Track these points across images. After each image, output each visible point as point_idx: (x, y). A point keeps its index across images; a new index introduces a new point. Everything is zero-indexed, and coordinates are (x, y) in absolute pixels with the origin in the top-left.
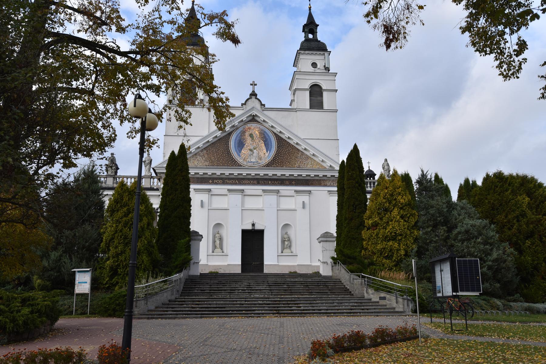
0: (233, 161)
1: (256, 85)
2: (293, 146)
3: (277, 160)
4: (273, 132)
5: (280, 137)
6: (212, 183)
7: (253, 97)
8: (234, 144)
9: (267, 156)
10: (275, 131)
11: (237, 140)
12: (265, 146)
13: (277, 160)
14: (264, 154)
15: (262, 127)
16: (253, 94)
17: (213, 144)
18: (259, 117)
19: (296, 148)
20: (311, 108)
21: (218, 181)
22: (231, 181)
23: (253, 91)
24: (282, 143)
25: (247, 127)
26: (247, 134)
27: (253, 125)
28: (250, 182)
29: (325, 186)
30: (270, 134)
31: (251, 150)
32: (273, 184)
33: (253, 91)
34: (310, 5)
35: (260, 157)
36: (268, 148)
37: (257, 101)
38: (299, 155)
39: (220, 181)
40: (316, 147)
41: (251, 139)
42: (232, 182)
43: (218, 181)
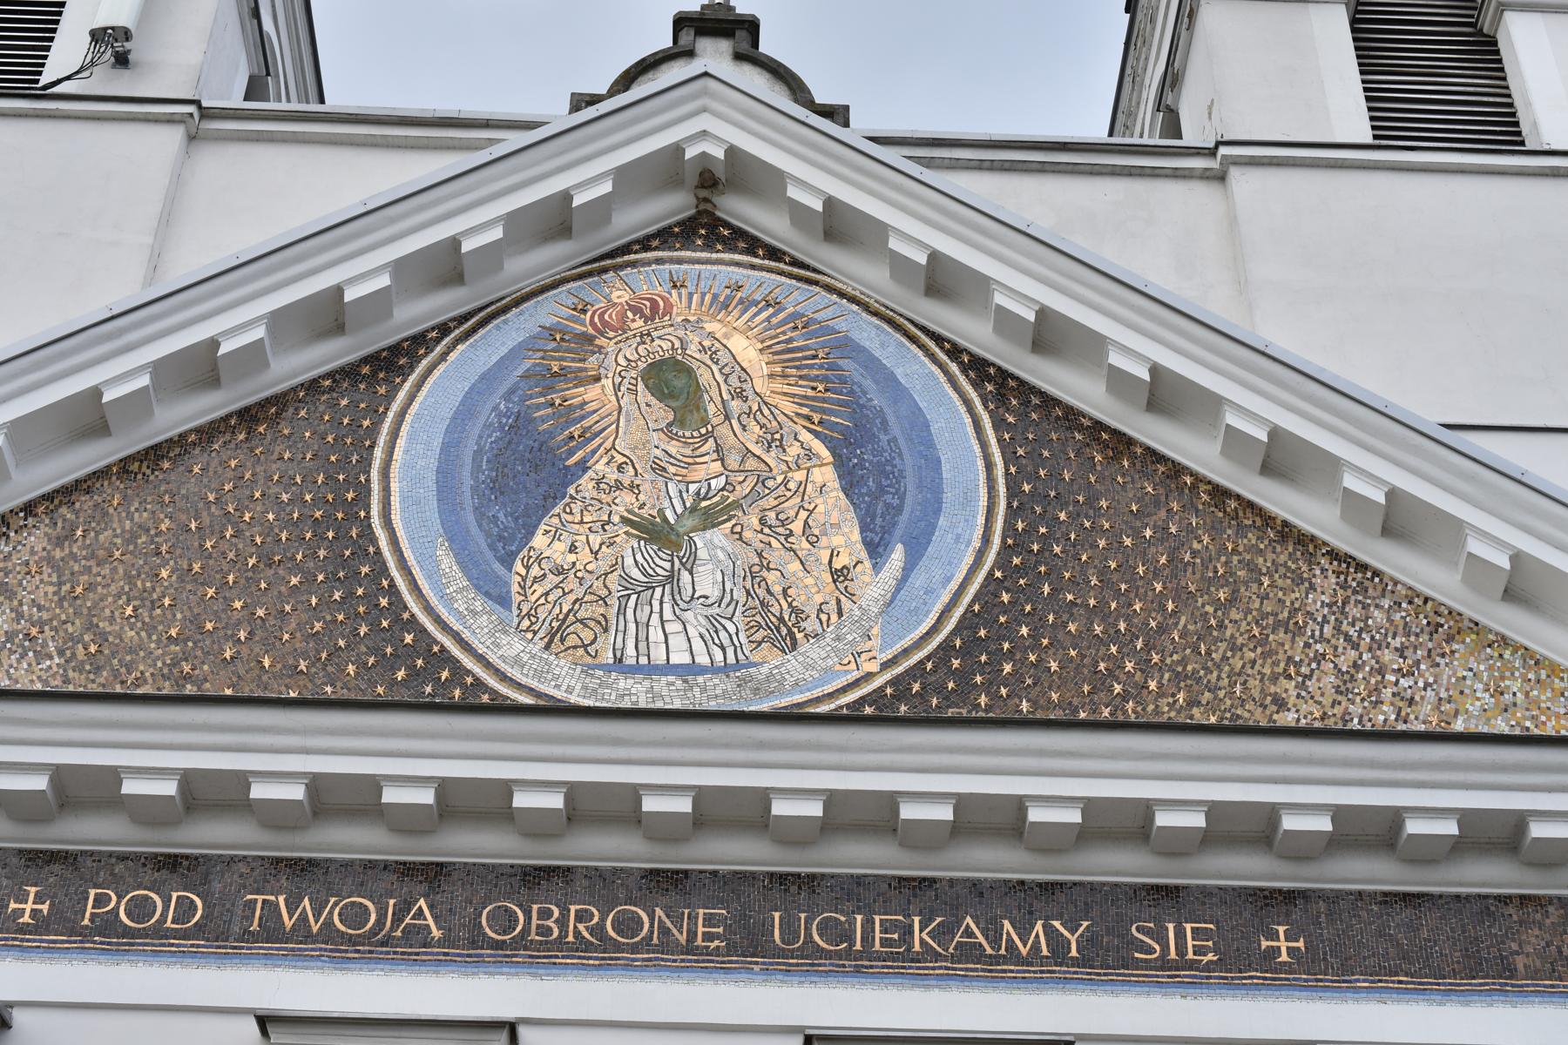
0: (404, 655)
2: (1220, 494)
3: (1019, 646)
4: (955, 352)
5: (1049, 401)
6: (41, 925)
7: (714, 56)
8: (429, 464)
10: (975, 333)
11: (485, 415)
12: (850, 483)
13: (1019, 646)
14: (840, 575)
15: (798, 298)
17: (154, 454)
19: (1267, 519)
21: (140, 909)
22: (334, 912)
25: (621, 296)
28: (628, 925)
31: (655, 532)
32: (969, 953)
35: (779, 607)
38: (1315, 602)
39: (163, 907)
41: (662, 414)
42: (355, 916)
43: (140, 909)
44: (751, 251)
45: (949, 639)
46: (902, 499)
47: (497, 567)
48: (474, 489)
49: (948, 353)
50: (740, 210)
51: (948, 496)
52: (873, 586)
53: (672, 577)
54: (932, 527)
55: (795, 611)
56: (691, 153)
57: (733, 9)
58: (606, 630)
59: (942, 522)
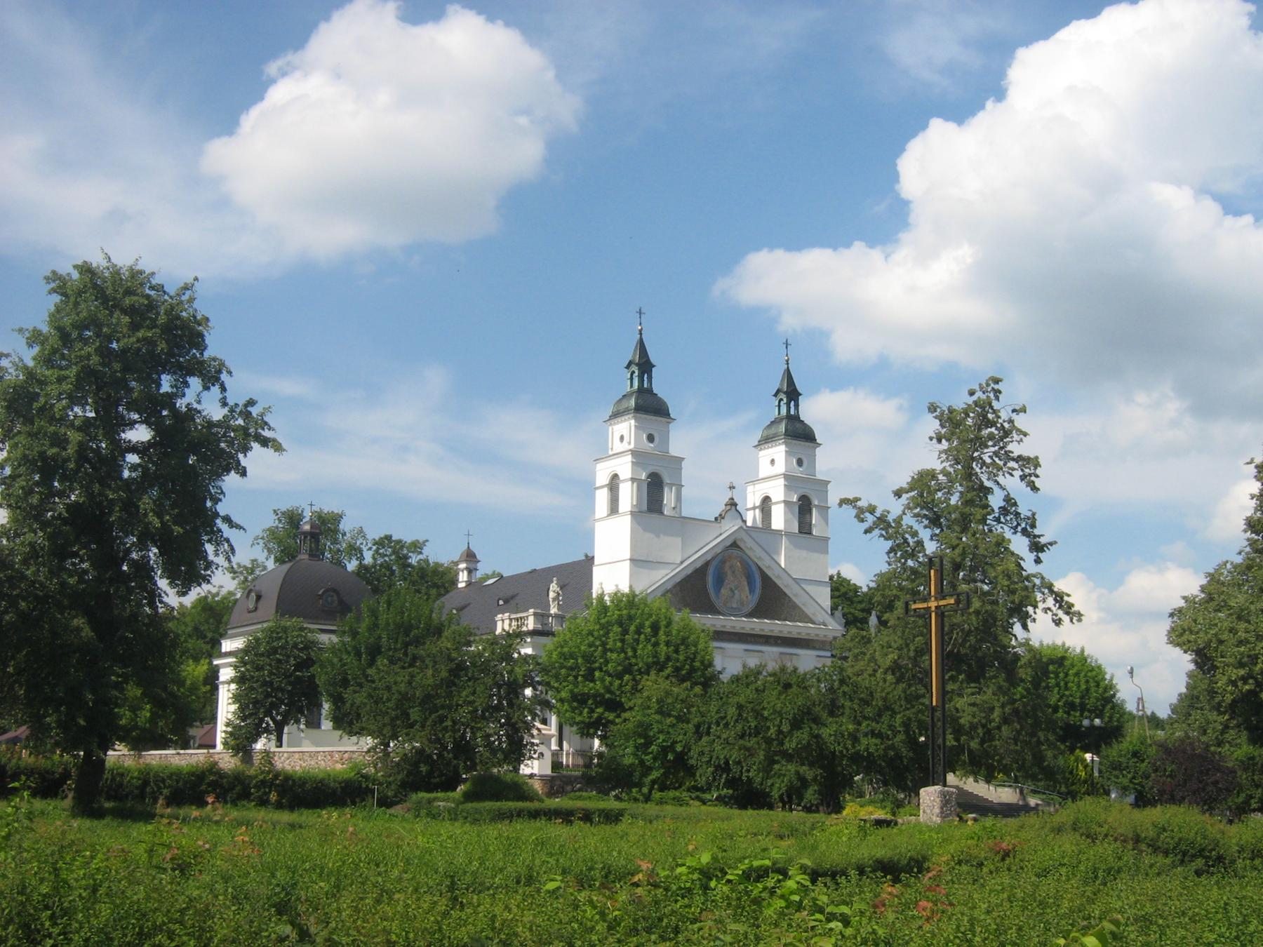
1: (734, 488)
9: (752, 600)
10: (760, 564)
12: (748, 583)
16: (732, 504)
18: (745, 542)
20: (800, 532)
24: (768, 583)
26: (728, 564)
27: (735, 552)
29: (814, 648)
30: (754, 568)
33: (732, 499)
34: (787, 355)
36: (752, 590)
37: (736, 512)
40: (810, 593)
50: (739, 543)
52: (749, 597)
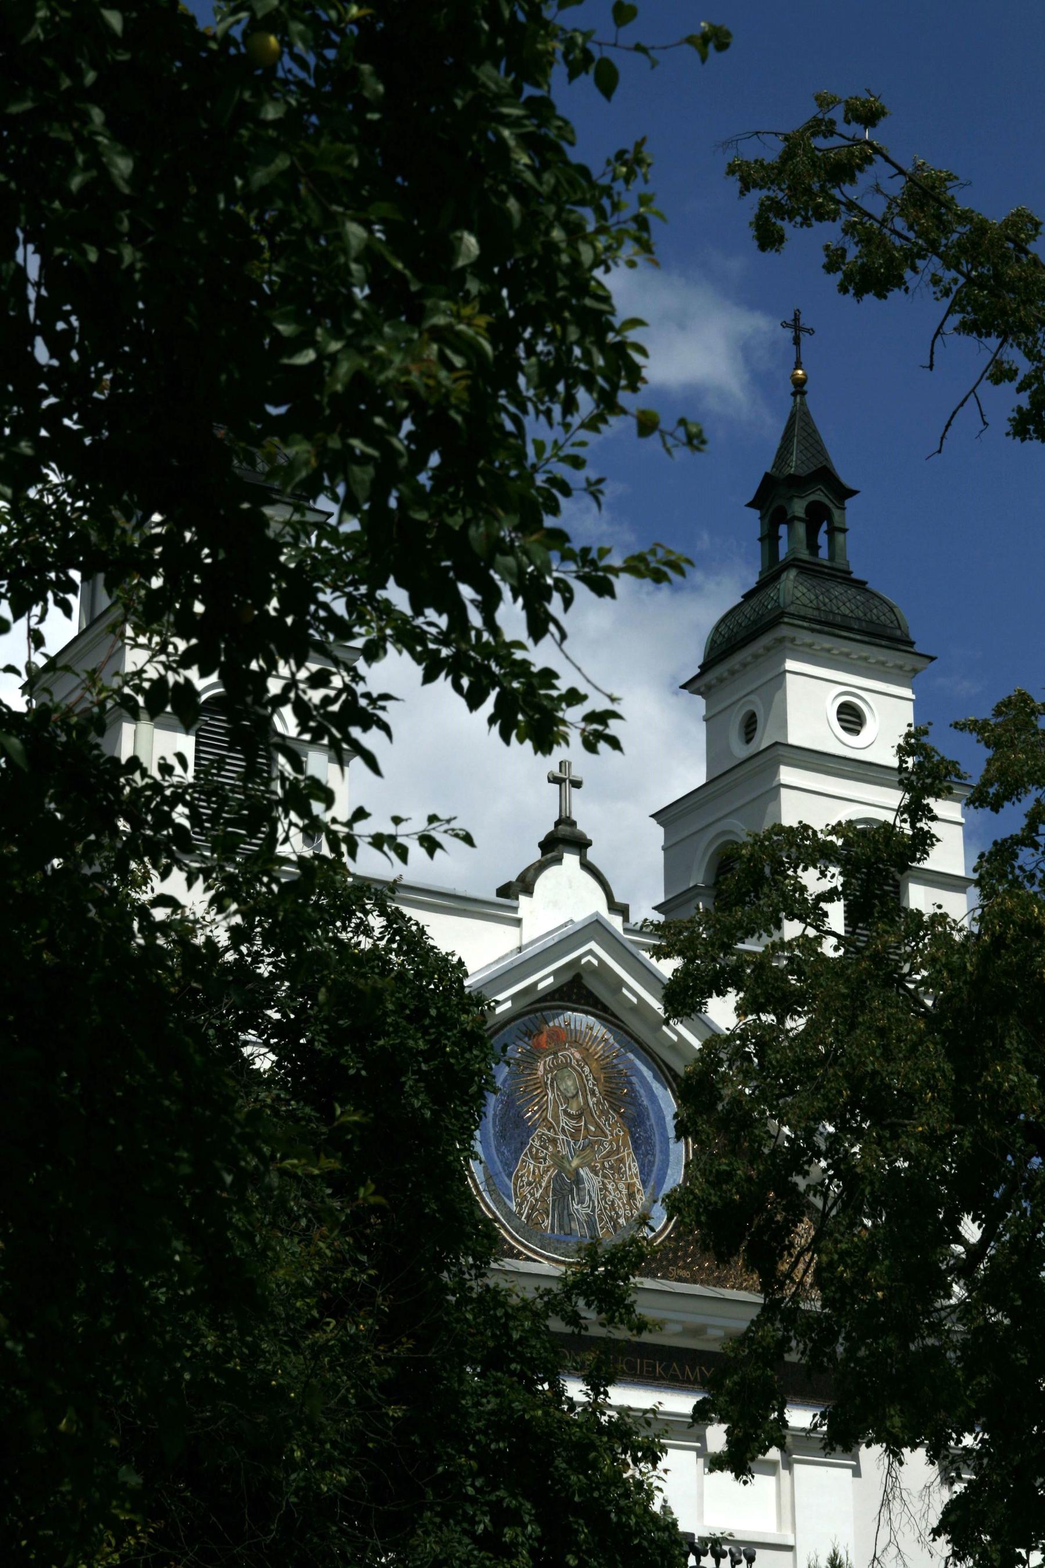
1: (577, 784)
12: (636, 1149)
14: (631, 1196)
23: (565, 821)
33: (565, 821)
44: (595, 1006)
45: (670, 1233)
46: (654, 1155)
47: (506, 1179)
48: (495, 1135)
49: (673, 1077)
51: (671, 1158)
53: (571, 1191)
54: (665, 1173)
55: (617, 1213)
56: (583, 961)
57: (574, 824)
58: (548, 1216)
59: (669, 1172)
